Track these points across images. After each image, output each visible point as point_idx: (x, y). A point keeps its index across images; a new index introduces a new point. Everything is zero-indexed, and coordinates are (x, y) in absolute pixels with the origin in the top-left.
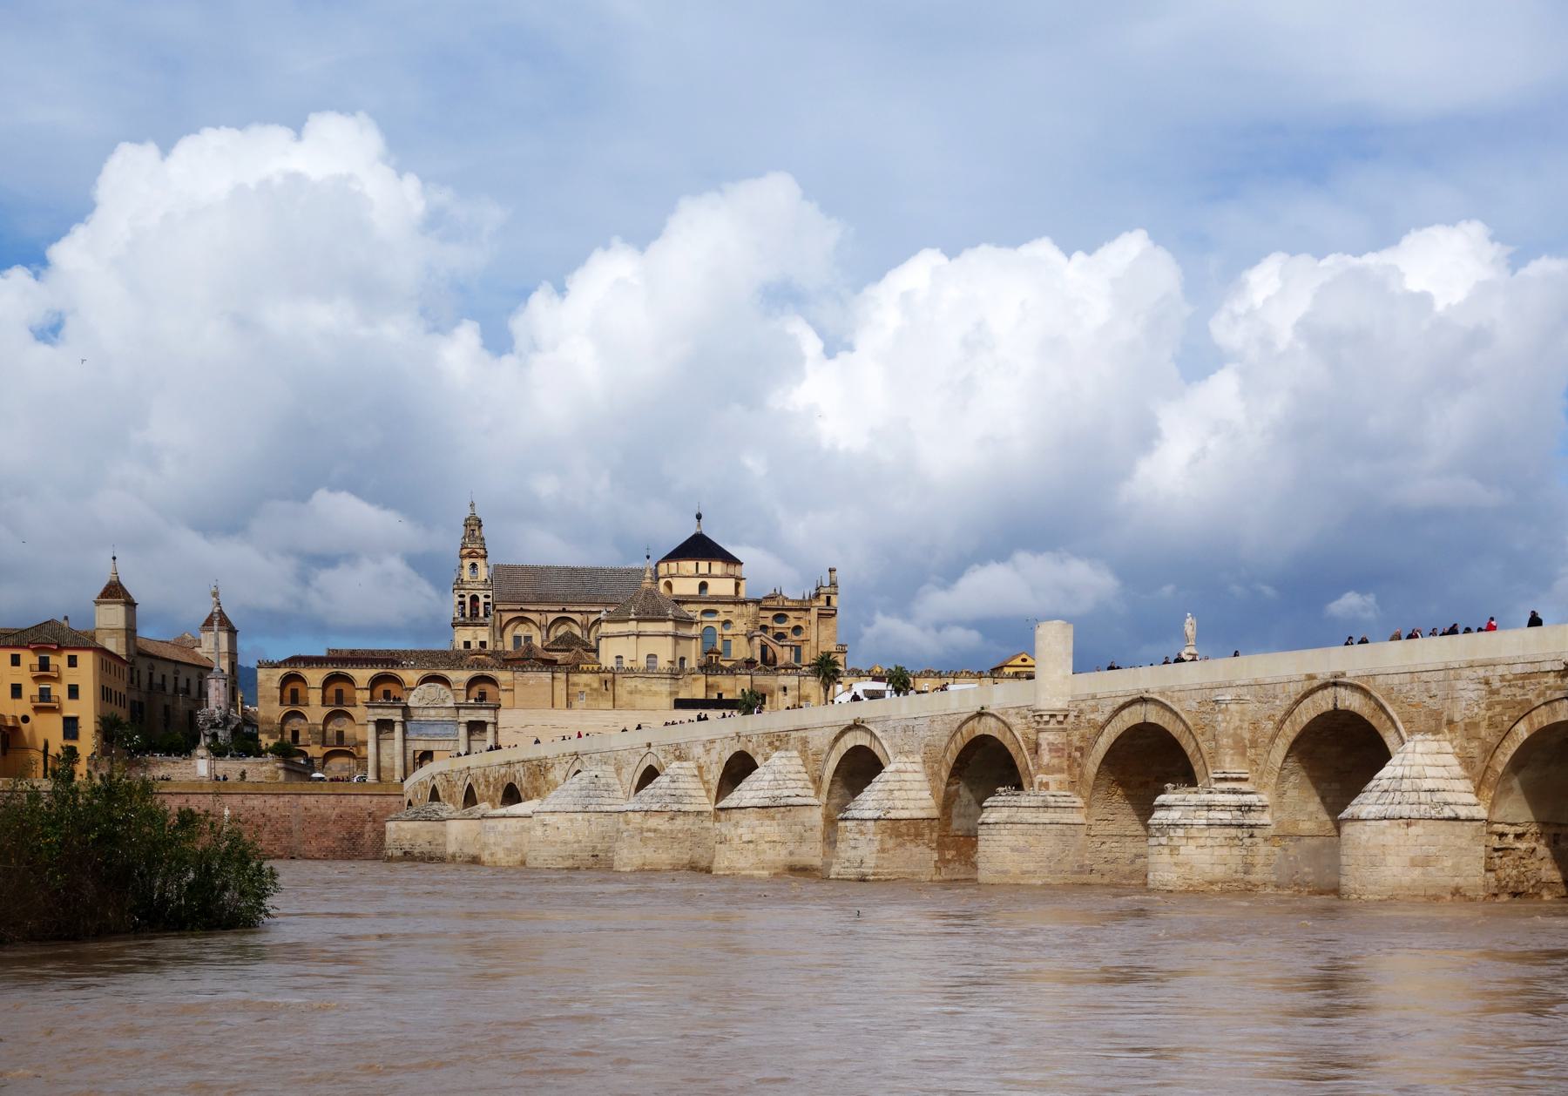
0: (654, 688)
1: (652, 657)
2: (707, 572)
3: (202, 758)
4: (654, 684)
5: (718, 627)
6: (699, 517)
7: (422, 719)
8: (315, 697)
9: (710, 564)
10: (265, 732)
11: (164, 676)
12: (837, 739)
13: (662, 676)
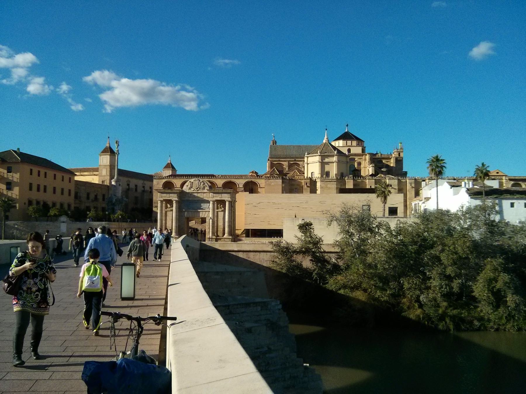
0: (329, 186)
1: (328, 174)
2: (351, 145)
3: (64, 222)
4: (329, 184)
6: (347, 126)
7: (190, 199)
9: (352, 142)
11: (136, 186)
13: (332, 181)
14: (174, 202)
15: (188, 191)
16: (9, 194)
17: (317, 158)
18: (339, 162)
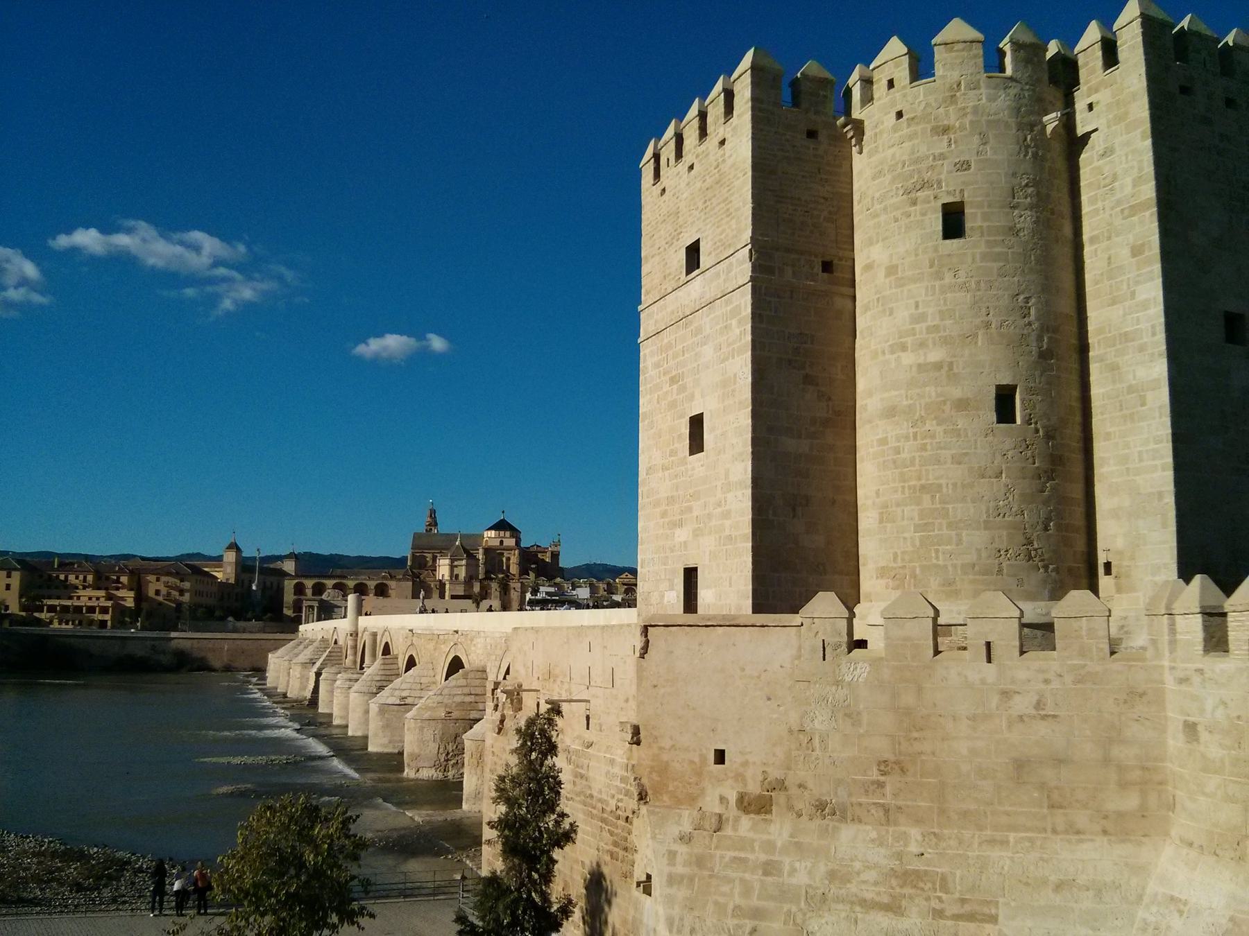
1: (457, 576)
5: (504, 559)
6: (503, 512)
8: (309, 592)
10: (286, 607)
12: (333, 635)
14: (316, 608)
15: (326, 599)
16: (181, 598)
17: (447, 561)
18: (467, 565)
